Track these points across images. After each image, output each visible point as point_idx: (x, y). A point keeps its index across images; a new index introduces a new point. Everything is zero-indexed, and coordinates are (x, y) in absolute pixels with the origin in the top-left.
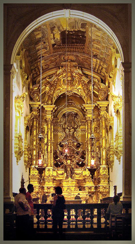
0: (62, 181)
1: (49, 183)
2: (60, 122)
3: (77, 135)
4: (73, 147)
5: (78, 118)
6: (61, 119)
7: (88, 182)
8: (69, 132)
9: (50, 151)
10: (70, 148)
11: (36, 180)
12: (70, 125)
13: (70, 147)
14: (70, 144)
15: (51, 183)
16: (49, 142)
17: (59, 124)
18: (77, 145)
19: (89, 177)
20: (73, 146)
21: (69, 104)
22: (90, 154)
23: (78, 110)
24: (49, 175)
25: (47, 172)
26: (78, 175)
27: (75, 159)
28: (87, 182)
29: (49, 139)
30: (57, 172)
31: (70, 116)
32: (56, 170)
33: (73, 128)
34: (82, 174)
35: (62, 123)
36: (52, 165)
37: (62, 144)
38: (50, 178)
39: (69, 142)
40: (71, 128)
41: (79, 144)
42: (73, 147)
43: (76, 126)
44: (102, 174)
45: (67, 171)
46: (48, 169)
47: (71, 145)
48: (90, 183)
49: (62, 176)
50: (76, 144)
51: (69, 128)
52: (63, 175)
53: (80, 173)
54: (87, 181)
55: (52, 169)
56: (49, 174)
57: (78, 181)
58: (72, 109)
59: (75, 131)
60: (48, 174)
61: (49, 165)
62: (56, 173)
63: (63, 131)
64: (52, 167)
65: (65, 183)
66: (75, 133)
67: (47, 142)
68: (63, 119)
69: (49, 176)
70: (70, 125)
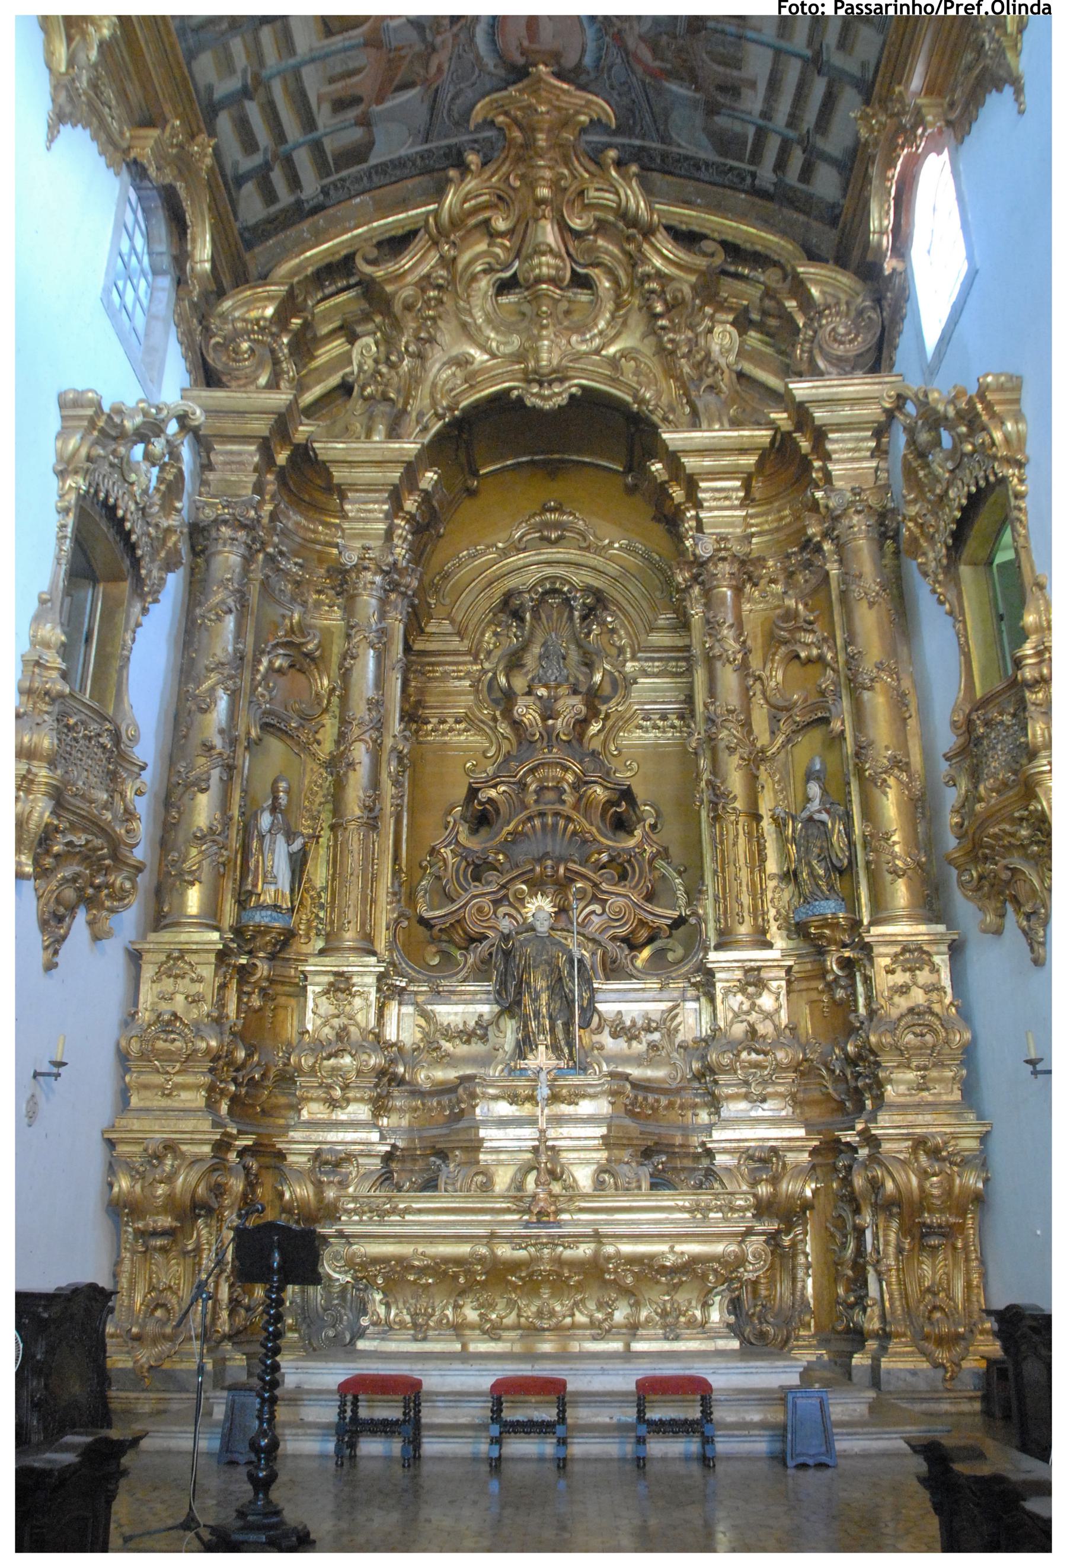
0: (473, 1096)
1: (341, 1116)
2: (476, 658)
3: (605, 744)
5: (613, 631)
6: (483, 635)
7: (743, 1105)
8: (544, 719)
9: (358, 812)
10: (555, 825)
11: (189, 1079)
12: (552, 674)
13: (557, 814)
14: (550, 795)
15: (361, 1111)
16: (356, 731)
17: (468, 673)
18: (610, 803)
19: (751, 1050)
20: (576, 807)
21: (548, 540)
22: (742, 840)
24: (342, 1034)
25: (326, 1006)
26: (636, 1037)
27: (597, 908)
28: (729, 1097)
29: (360, 710)
30: (424, 1014)
31: (549, 618)
32: (420, 999)
34: (666, 1024)
35: (487, 665)
36: (381, 946)
37: (482, 796)
38: (347, 1060)
39: (546, 779)
40: (563, 690)
41: (627, 795)
42: (575, 815)
43: (598, 678)
44: (895, 1013)
45: (518, 1003)
46: (332, 979)
47: (563, 802)
48: (759, 1113)
49: (476, 1048)
50: (600, 793)
51: (542, 692)
52: (484, 1038)
53: (656, 1017)
54: (730, 1091)
55: (371, 980)
56: (336, 1022)
57: (636, 1101)
59: (593, 713)
60: (336, 1022)
61: (350, 937)
62: (423, 1022)
63: (495, 719)
64: (373, 960)
65: (503, 1109)
66: (595, 727)
67: (341, 737)
68: (495, 634)
69: (339, 1037)
70: (552, 674)
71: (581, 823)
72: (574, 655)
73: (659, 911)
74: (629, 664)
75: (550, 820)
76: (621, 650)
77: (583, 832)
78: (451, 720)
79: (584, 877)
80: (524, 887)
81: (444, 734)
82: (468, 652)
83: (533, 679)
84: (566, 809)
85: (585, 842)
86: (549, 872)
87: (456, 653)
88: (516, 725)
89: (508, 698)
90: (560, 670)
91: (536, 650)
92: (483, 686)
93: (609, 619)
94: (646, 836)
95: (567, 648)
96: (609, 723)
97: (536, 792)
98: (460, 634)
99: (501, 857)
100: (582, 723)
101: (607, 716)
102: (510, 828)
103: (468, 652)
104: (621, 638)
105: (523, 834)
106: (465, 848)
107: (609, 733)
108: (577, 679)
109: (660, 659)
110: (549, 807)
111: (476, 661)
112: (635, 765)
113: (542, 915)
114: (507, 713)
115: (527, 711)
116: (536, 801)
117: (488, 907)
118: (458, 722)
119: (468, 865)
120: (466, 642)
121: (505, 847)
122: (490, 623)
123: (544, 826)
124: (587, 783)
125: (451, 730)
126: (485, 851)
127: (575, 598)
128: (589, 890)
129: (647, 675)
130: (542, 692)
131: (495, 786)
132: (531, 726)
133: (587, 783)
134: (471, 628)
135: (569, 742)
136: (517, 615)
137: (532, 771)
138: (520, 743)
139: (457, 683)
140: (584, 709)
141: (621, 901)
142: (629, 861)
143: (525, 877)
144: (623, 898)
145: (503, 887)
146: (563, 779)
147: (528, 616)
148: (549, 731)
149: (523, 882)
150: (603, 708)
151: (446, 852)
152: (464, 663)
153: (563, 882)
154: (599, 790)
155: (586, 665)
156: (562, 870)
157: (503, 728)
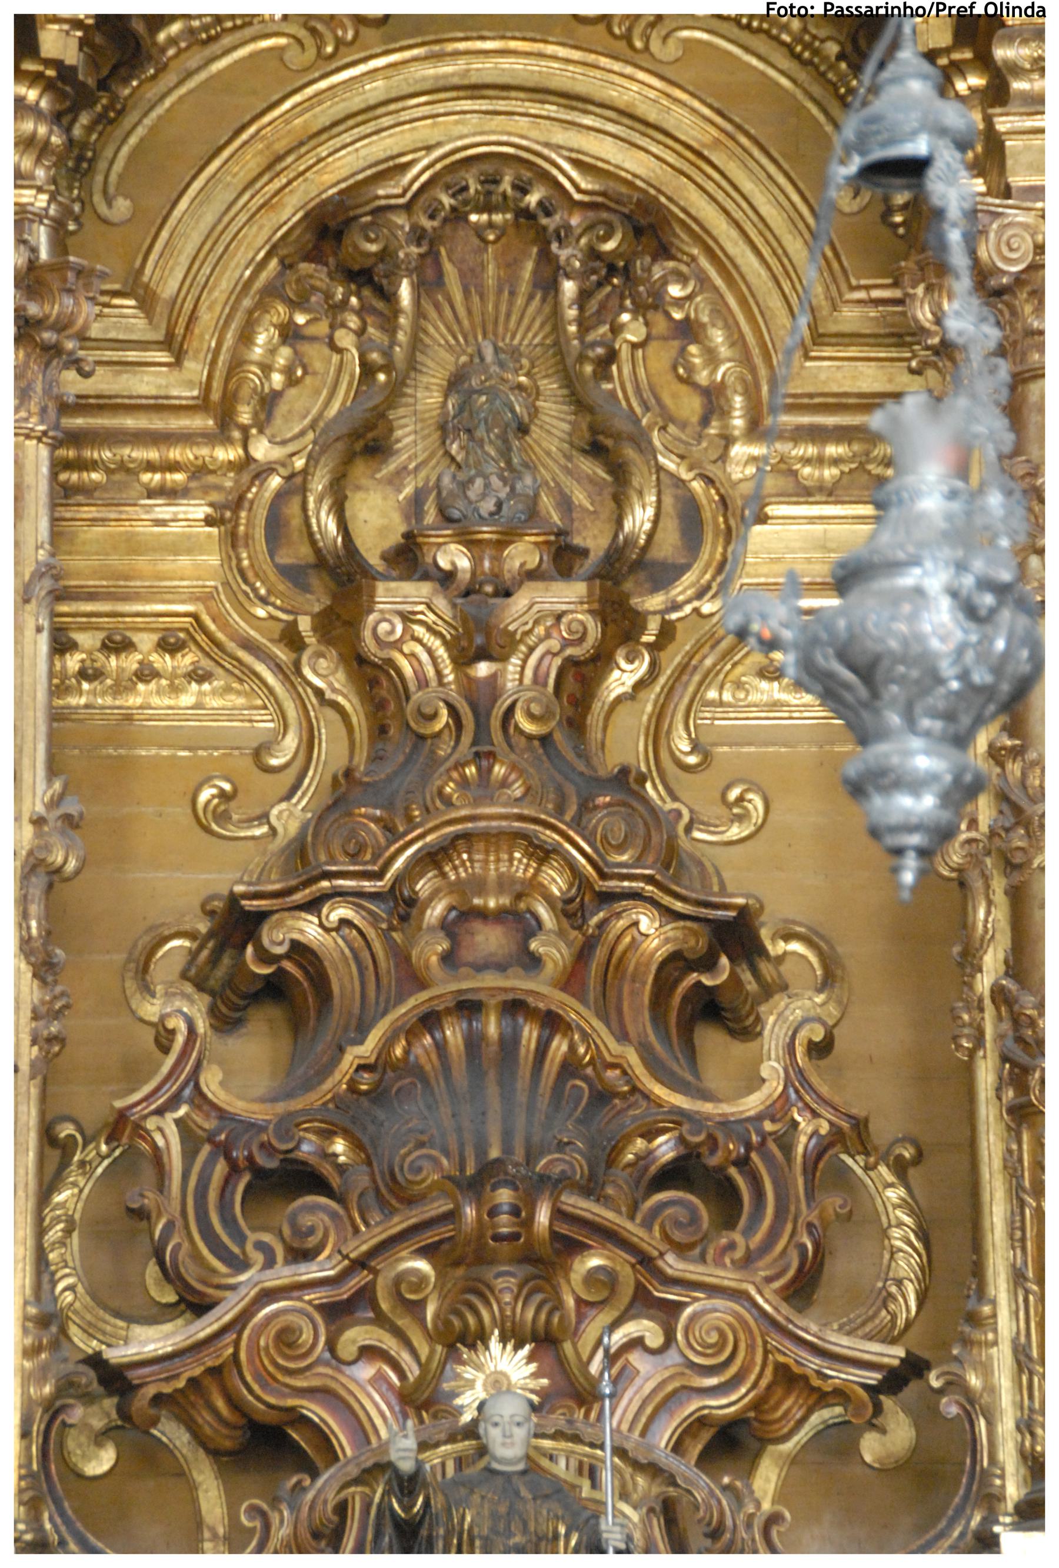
2: (226, 419)
4: (573, 1010)
5: (688, 331)
6: (246, 337)
8: (465, 655)
10: (509, 1044)
12: (486, 494)
13: (515, 1007)
14: (490, 940)
17: (199, 471)
18: (677, 962)
20: (572, 980)
23: (688, 121)
31: (471, 279)
33: (563, 558)
35: (262, 450)
37: (276, 937)
39: (479, 886)
40: (522, 554)
41: (736, 935)
42: (573, 1010)
43: (639, 518)
47: (533, 962)
50: (650, 933)
51: (454, 557)
58: (539, 92)
59: (620, 625)
63: (292, 639)
66: (622, 677)
68: (289, 334)
70: (486, 494)
71: (593, 1035)
72: (554, 422)
73: (842, 1343)
74: (739, 450)
75: (492, 1027)
76: (714, 401)
77: (601, 1063)
78: (145, 641)
79: (609, 1236)
80: (423, 1265)
81: (122, 687)
82: (202, 405)
83: (417, 501)
84: (541, 988)
85: (602, 1096)
86: (505, 1224)
87: (159, 406)
88: (370, 674)
89: (343, 580)
90: (511, 473)
91: (428, 396)
92: (254, 521)
93: (675, 291)
94: (795, 1078)
95: (532, 393)
96: (673, 658)
97: (446, 927)
98: (175, 345)
99: (339, 1146)
100: (581, 676)
101: (667, 632)
102: (367, 1049)
103: (202, 405)
104: (712, 358)
105: (408, 1068)
106: (222, 1114)
107: (672, 692)
108: (566, 504)
109: (841, 434)
110: (490, 980)
111: (221, 435)
112: (756, 801)
113: (510, 1409)
114: (341, 625)
115: (411, 627)
116: (448, 959)
117: (311, 1333)
118: (169, 646)
119: (234, 1169)
120: (195, 368)
121: (347, 1114)
122: (272, 292)
123: (474, 1043)
124: (608, 898)
125: (146, 674)
126: (287, 1125)
127: (563, 235)
128: (627, 1275)
129: (805, 493)
130: (454, 557)
131: (313, 905)
132: (423, 682)
133: (608, 898)
134: (207, 318)
135: (545, 740)
136: (370, 279)
137: (433, 858)
138: (380, 731)
139: (163, 511)
140: (594, 629)
141: (720, 1312)
142: (743, 1163)
143: (430, 1237)
144: (723, 1294)
145: (360, 1264)
146: (533, 887)
147: (405, 292)
148: (481, 699)
149: (425, 1252)
150: (654, 602)
151: (166, 1134)
152: (186, 438)
153: (546, 1251)
154: (647, 922)
155: (596, 450)
156: (543, 1216)
157: (323, 673)
